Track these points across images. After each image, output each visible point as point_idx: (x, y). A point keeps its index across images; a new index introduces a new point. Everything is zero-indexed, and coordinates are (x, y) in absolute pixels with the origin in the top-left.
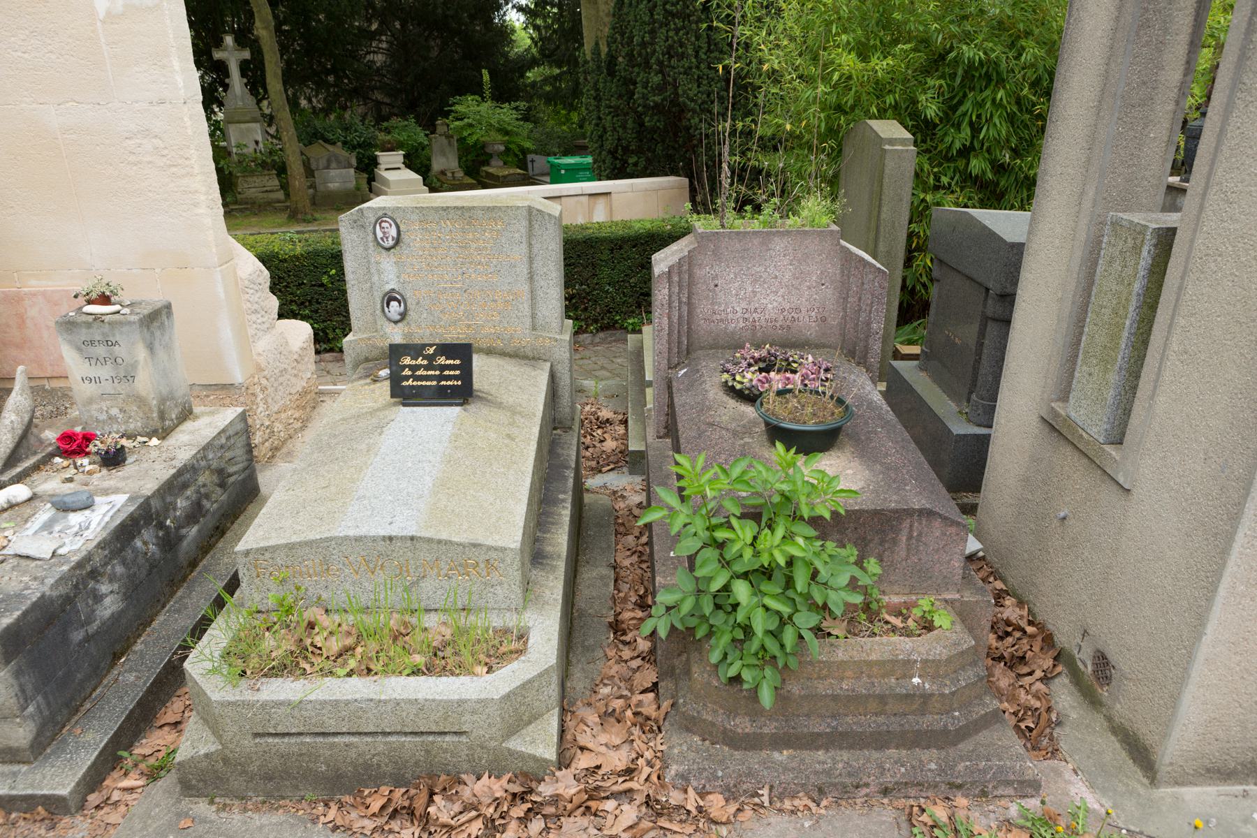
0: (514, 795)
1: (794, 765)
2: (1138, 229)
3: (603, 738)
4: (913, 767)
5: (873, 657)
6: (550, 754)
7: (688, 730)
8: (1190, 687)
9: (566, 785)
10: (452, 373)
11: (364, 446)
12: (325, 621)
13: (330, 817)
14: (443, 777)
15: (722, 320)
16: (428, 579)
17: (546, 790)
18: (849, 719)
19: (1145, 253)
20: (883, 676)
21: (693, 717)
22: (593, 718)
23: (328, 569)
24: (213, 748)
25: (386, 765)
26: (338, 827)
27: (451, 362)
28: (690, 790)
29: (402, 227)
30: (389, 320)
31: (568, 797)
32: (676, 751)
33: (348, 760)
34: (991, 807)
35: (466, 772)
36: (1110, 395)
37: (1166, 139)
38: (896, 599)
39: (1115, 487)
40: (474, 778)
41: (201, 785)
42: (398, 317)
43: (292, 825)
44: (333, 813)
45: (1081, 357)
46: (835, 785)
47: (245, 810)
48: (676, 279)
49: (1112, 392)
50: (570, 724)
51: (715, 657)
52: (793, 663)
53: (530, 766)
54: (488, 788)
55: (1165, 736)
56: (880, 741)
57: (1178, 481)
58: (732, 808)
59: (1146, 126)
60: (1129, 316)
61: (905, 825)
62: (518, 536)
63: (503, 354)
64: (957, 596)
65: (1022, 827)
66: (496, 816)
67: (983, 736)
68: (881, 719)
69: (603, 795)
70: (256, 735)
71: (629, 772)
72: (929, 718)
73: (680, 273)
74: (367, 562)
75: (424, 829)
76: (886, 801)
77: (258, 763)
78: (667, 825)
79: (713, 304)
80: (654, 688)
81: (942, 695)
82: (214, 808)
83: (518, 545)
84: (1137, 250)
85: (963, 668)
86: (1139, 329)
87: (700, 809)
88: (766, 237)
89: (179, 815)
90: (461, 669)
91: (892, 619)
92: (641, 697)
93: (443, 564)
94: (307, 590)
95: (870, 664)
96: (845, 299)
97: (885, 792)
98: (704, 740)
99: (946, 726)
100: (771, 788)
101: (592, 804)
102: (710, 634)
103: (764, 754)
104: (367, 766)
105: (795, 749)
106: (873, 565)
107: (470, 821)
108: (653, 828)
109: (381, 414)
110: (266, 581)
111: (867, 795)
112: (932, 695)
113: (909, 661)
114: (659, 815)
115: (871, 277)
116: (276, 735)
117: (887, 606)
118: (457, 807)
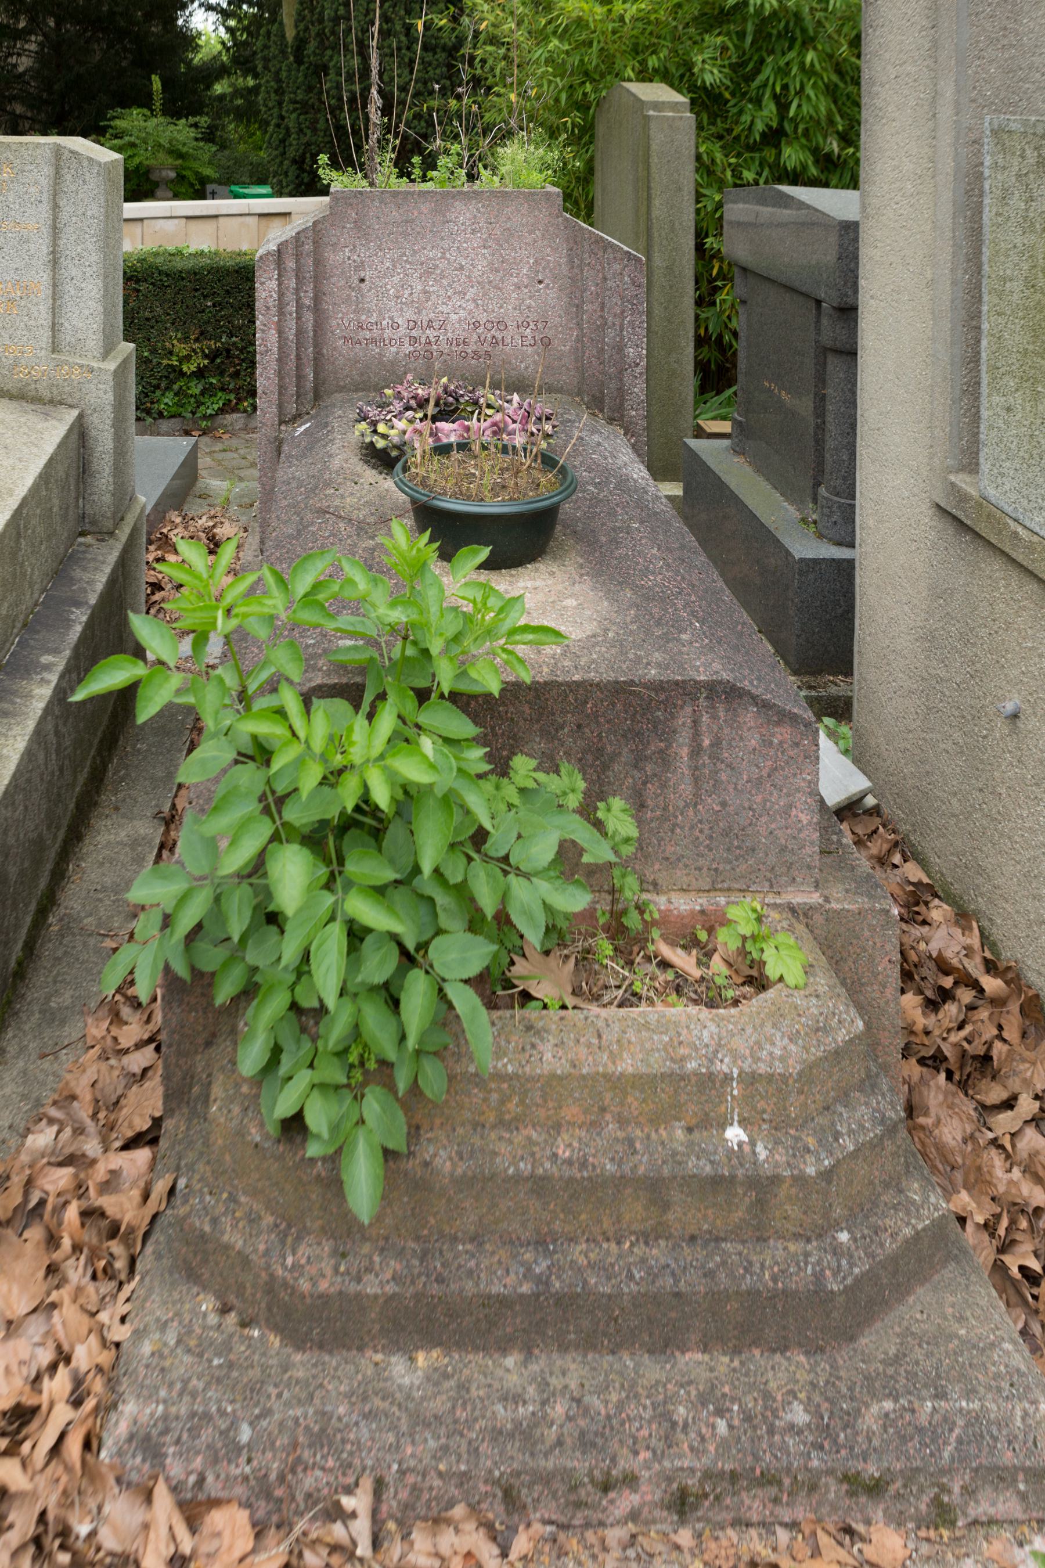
15: (373, 340)
48: (291, 264)
73: (298, 257)
79: (357, 312)
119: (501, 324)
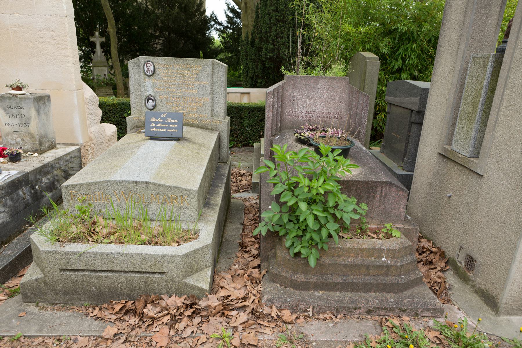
0: (187, 305)
1: (325, 297)
2: (486, 57)
3: (233, 285)
4: (382, 300)
5: (364, 247)
6: (205, 286)
7: (274, 281)
8: (516, 262)
9: (213, 301)
10: (173, 126)
11: (130, 152)
12: (102, 222)
13: (95, 314)
14: (153, 296)
15: (296, 116)
16: (153, 204)
17: (202, 304)
18: (352, 277)
19: (489, 66)
20: (368, 257)
21: (277, 274)
22: (228, 277)
23: (105, 197)
24: (39, 276)
25: (125, 289)
26: (98, 318)
27: (173, 121)
28: (274, 307)
29: (156, 67)
30: (148, 109)
31: (213, 306)
32: (268, 290)
33: (106, 285)
34: (420, 321)
35: (164, 294)
36: (473, 134)
37: (496, 24)
38: (374, 226)
39: (475, 176)
40: (168, 297)
41: (32, 296)
42: (152, 108)
43: (75, 317)
44: (96, 312)
45: (458, 121)
46: (344, 307)
47: (53, 310)
48: (276, 95)
49: (474, 133)
50: (217, 279)
51: (288, 244)
52: (326, 247)
53: (196, 292)
54: (174, 302)
55: (503, 289)
56: (366, 288)
57: (507, 165)
58: (294, 316)
59: (487, 17)
60: (482, 96)
61: (378, 328)
62: (198, 186)
63: (198, 127)
64: (402, 226)
65: (435, 330)
66: (177, 314)
67: (415, 289)
68: (367, 277)
69: (231, 308)
70: (62, 270)
71: (245, 299)
72: (390, 278)
73: (278, 93)
74: (125, 194)
75: (140, 320)
76: (369, 317)
77: (61, 285)
78: (262, 323)
79: (292, 108)
80: (259, 266)
81: (396, 266)
82: (38, 308)
83: (197, 189)
84: (485, 66)
85: (406, 255)
86: (486, 102)
87: (278, 316)
88: (317, 79)
89: (20, 311)
90: (166, 243)
91: (372, 235)
92: (252, 270)
93: (160, 197)
94: (95, 207)
95: (362, 250)
96: (350, 109)
97: (369, 312)
98: (281, 286)
99: (398, 281)
100: (314, 308)
101: (226, 312)
102: (287, 234)
103: (310, 292)
104: (115, 289)
105: (325, 291)
106: (364, 206)
107: (164, 316)
108: (254, 324)
109: (140, 143)
110: (75, 202)
111: (360, 314)
112: (391, 266)
113: (381, 249)
114: (258, 318)
115: (362, 98)
116: (72, 270)
117: (370, 229)
118: (158, 309)
119: (329, 113)
